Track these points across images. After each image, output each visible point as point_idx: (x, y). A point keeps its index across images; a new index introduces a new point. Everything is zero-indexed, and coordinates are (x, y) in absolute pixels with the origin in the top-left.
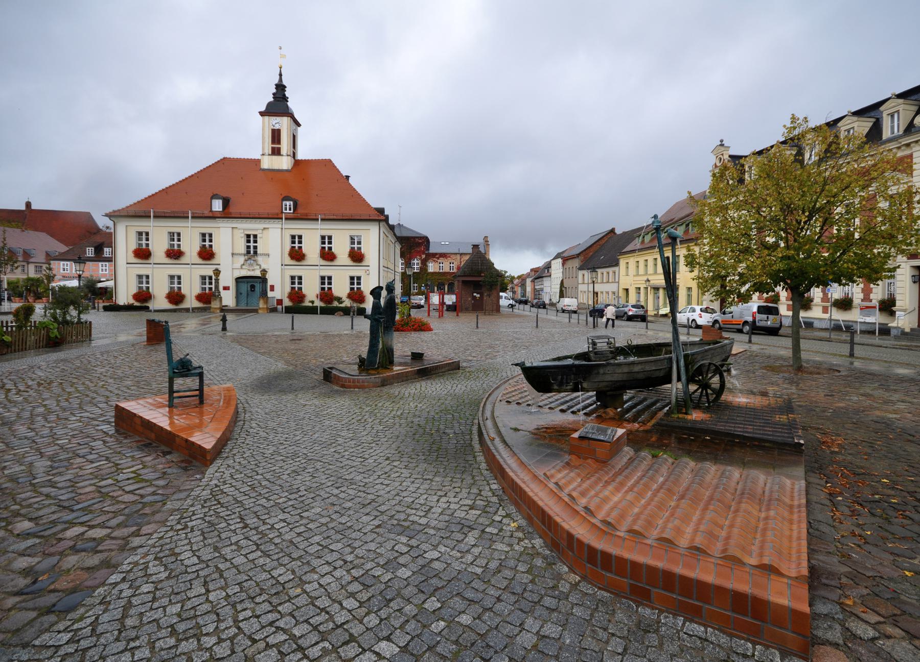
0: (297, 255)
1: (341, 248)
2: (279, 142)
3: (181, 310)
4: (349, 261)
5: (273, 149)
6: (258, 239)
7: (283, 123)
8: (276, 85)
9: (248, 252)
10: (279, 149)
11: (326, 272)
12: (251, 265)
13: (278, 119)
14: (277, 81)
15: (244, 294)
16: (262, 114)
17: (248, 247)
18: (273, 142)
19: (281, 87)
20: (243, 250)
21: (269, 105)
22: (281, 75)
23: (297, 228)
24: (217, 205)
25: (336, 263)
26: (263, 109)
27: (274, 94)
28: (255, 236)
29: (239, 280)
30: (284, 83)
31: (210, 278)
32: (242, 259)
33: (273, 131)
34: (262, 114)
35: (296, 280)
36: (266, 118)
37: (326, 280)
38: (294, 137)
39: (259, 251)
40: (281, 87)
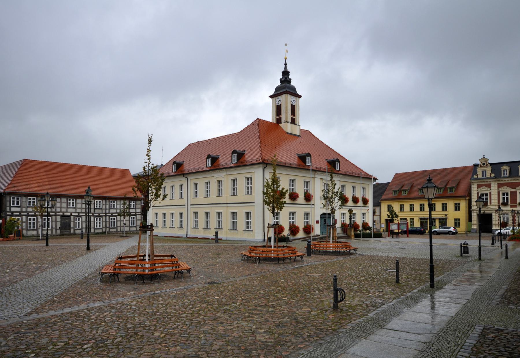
7: (286, 100)
8: (282, 72)
13: (280, 98)
14: (283, 70)
16: (271, 97)
18: (277, 115)
19: (286, 73)
21: (277, 89)
22: (286, 64)
26: (272, 92)
27: (281, 80)
30: (289, 70)
34: (271, 97)
36: (274, 99)
38: (293, 108)
40: (286, 73)
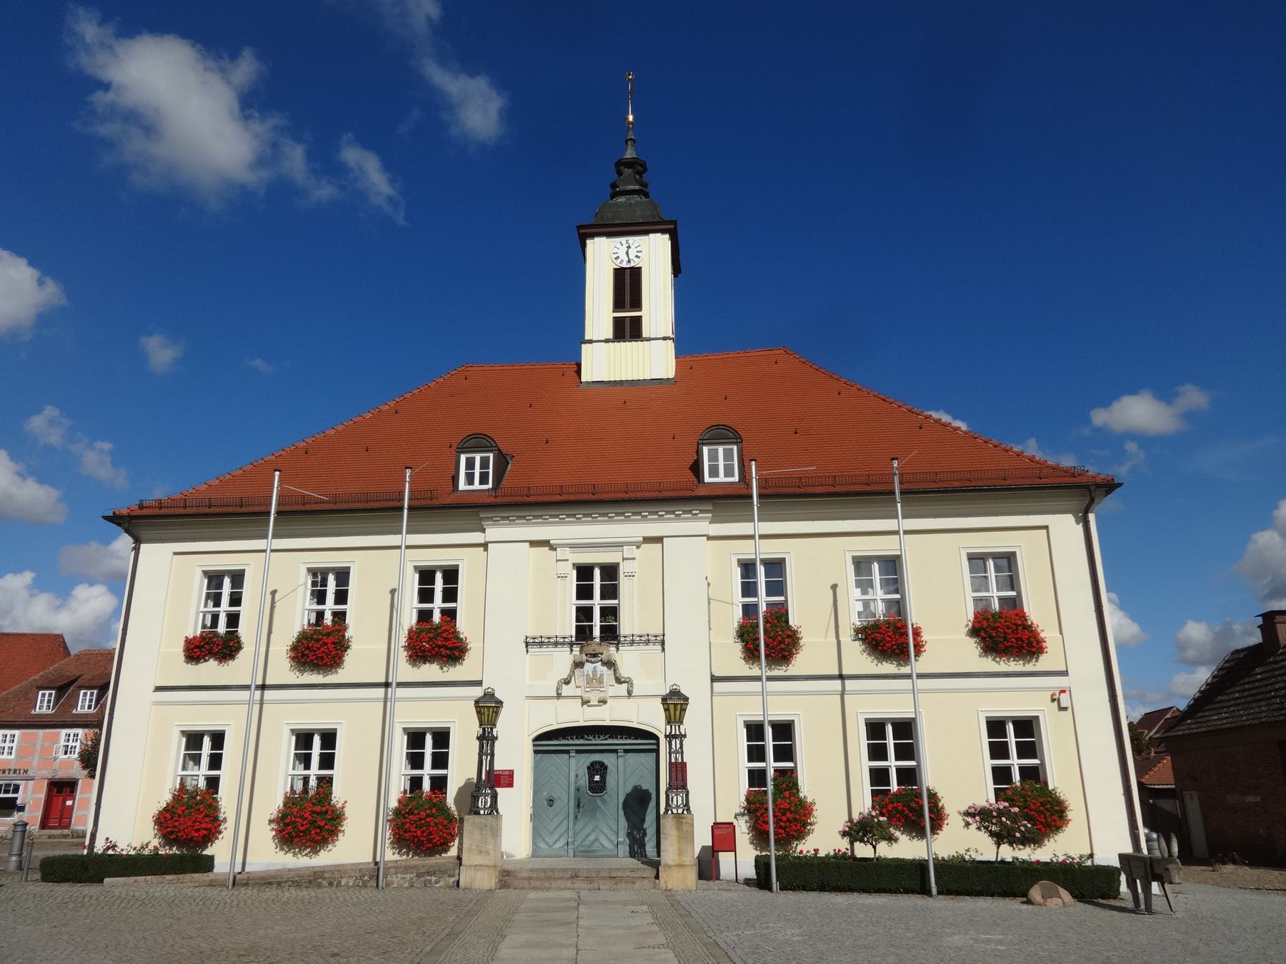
0: (769, 639)
1: (942, 605)
2: (636, 303)
3: (315, 878)
4: (969, 654)
5: (618, 323)
6: (624, 584)
9: (583, 633)
10: (637, 322)
11: (891, 702)
12: (595, 681)
13: (635, 241)
15: (565, 801)
17: (584, 614)
18: (618, 305)
20: (569, 627)
23: (763, 535)
24: (472, 475)
25: (922, 664)
28: (610, 572)
29: (551, 742)
31: (442, 738)
32: (563, 659)
33: (619, 273)
35: (773, 740)
37: (894, 738)
39: (626, 626)
